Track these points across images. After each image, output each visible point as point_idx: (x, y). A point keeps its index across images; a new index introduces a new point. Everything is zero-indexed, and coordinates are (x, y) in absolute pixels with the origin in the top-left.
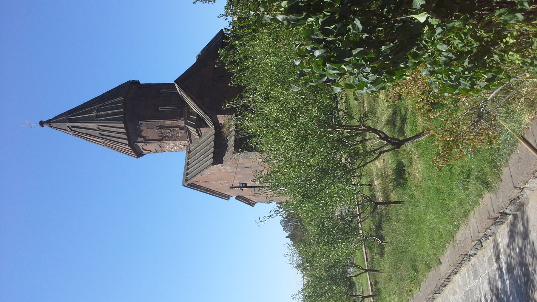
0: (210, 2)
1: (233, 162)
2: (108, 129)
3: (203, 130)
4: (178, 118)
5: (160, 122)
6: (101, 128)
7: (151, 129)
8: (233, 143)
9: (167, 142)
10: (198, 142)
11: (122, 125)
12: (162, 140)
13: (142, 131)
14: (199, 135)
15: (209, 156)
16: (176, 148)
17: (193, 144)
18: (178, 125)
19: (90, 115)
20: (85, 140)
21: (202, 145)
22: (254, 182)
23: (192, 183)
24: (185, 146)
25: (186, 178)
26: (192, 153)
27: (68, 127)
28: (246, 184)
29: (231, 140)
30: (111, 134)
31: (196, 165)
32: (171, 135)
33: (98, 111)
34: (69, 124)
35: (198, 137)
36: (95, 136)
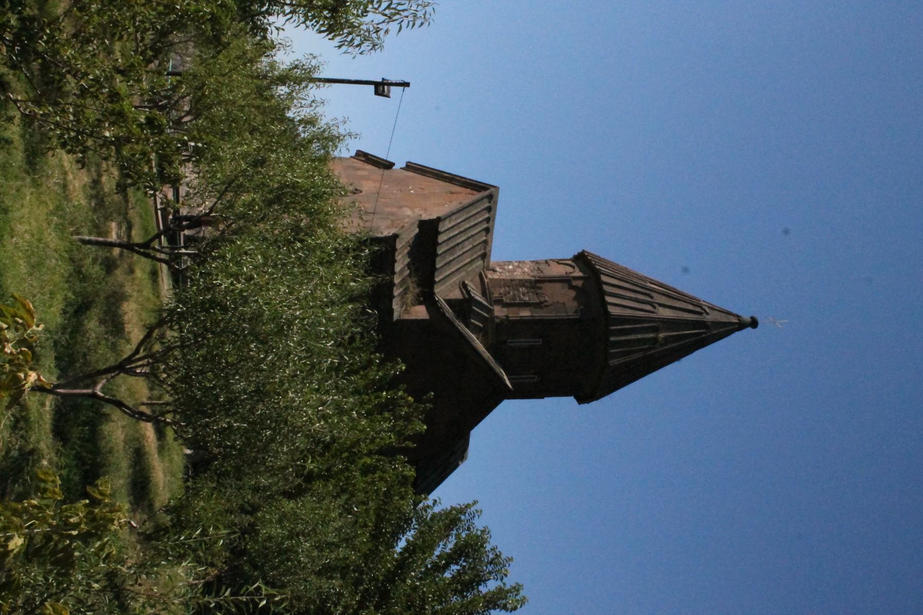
0: (443, 510)
1: (398, 222)
3: (457, 294)
4: (506, 323)
5: (539, 314)
6: (649, 308)
8: (398, 257)
9: (527, 277)
11: (612, 310)
12: (537, 281)
14: (464, 286)
15: (445, 238)
16: (511, 267)
17: (478, 270)
18: (505, 309)
20: (679, 288)
21: (459, 266)
22: (356, 190)
23: (479, 191)
24: (494, 271)
25: (492, 202)
26: (480, 253)
27: (707, 314)
28: (377, 93)
29: (402, 266)
30: (633, 295)
31: (472, 224)
32: (518, 291)
33: (655, 340)
34: (708, 318)
35: (466, 282)
36: (659, 293)
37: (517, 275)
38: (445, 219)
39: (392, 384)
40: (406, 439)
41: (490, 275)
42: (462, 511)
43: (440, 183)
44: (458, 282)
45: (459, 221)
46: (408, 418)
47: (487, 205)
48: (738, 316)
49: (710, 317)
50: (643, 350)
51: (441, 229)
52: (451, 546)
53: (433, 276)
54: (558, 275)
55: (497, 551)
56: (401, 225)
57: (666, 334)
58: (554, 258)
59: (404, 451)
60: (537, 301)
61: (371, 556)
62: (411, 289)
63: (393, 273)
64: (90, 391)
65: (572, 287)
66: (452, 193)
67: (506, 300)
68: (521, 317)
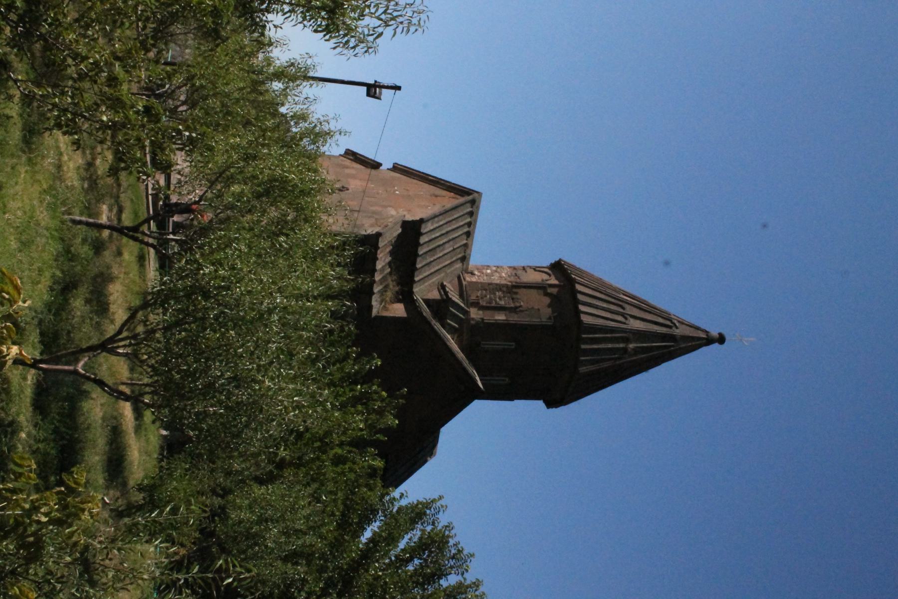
0: (409, 503)
1: (382, 221)
2: (608, 315)
3: (435, 295)
5: (514, 318)
6: (620, 318)
7: (533, 308)
9: (503, 282)
10: (447, 275)
11: (585, 319)
13: (549, 306)
14: (443, 287)
15: (427, 240)
16: (489, 271)
18: (481, 312)
19: (639, 345)
22: (343, 187)
23: (462, 196)
24: (472, 274)
25: (475, 207)
26: (460, 256)
27: (677, 328)
28: (368, 95)
29: (383, 264)
30: (605, 305)
32: (495, 294)
33: (625, 350)
35: (445, 283)
37: (494, 279)
38: (428, 220)
39: (367, 378)
40: (376, 433)
41: (468, 278)
42: (428, 505)
43: (426, 186)
44: (437, 283)
45: (441, 223)
46: (380, 412)
47: (469, 209)
48: (707, 332)
49: (680, 331)
50: (612, 359)
51: (423, 230)
52: (416, 539)
53: (413, 276)
54: (534, 281)
55: (459, 546)
56: (385, 223)
57: (636, 345)
58: (531, 265)
59: (375, 444)
60: (512, 305)
61: (337, 545)
62: (391, 286)
63: (374, 270)
64: (71, 368)
65: (546, 294)
66: (436, 196)
67: (483, 303)
68: (496, 320)
